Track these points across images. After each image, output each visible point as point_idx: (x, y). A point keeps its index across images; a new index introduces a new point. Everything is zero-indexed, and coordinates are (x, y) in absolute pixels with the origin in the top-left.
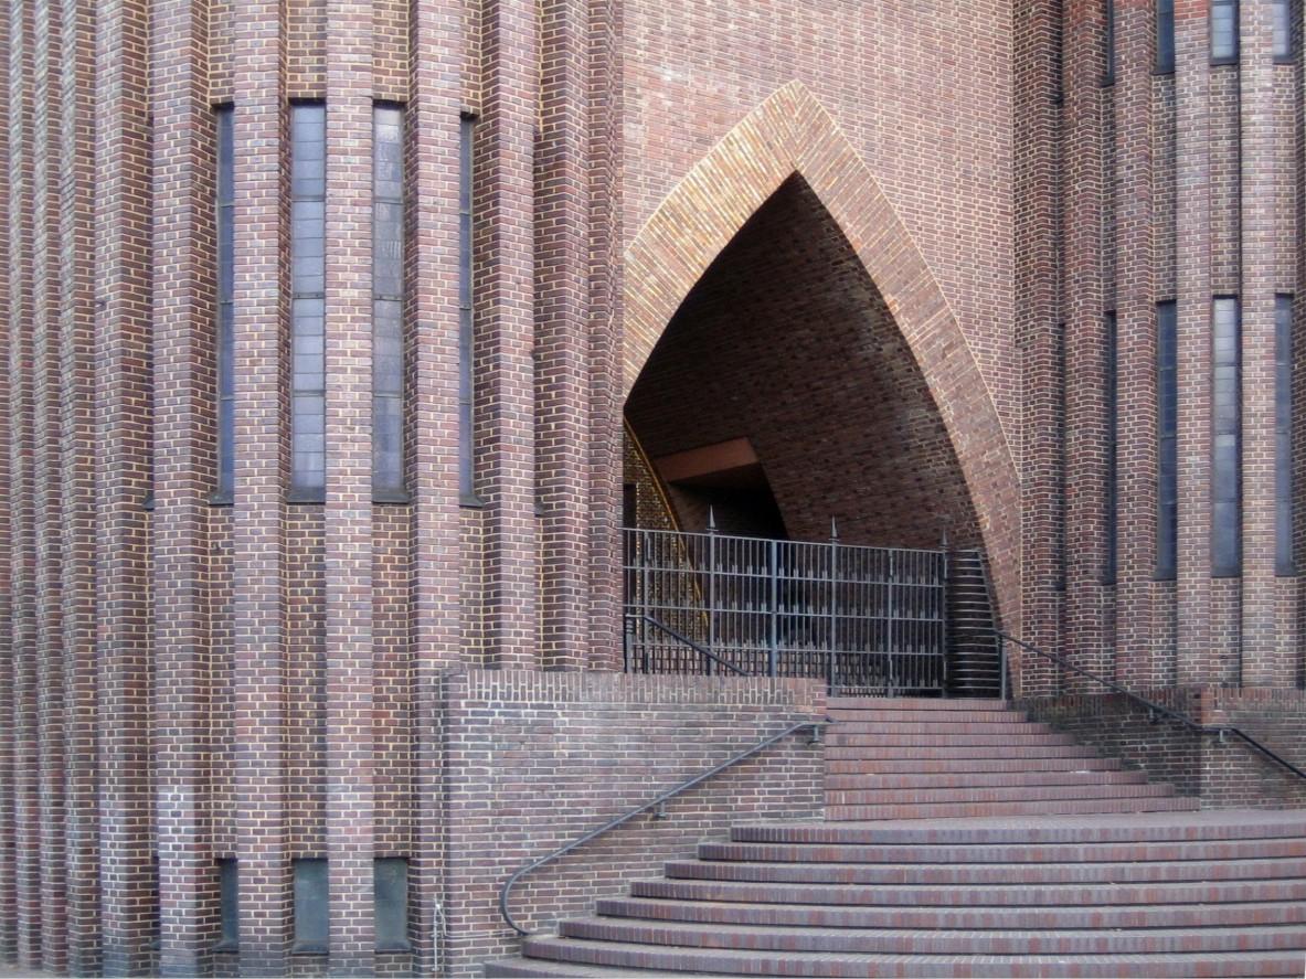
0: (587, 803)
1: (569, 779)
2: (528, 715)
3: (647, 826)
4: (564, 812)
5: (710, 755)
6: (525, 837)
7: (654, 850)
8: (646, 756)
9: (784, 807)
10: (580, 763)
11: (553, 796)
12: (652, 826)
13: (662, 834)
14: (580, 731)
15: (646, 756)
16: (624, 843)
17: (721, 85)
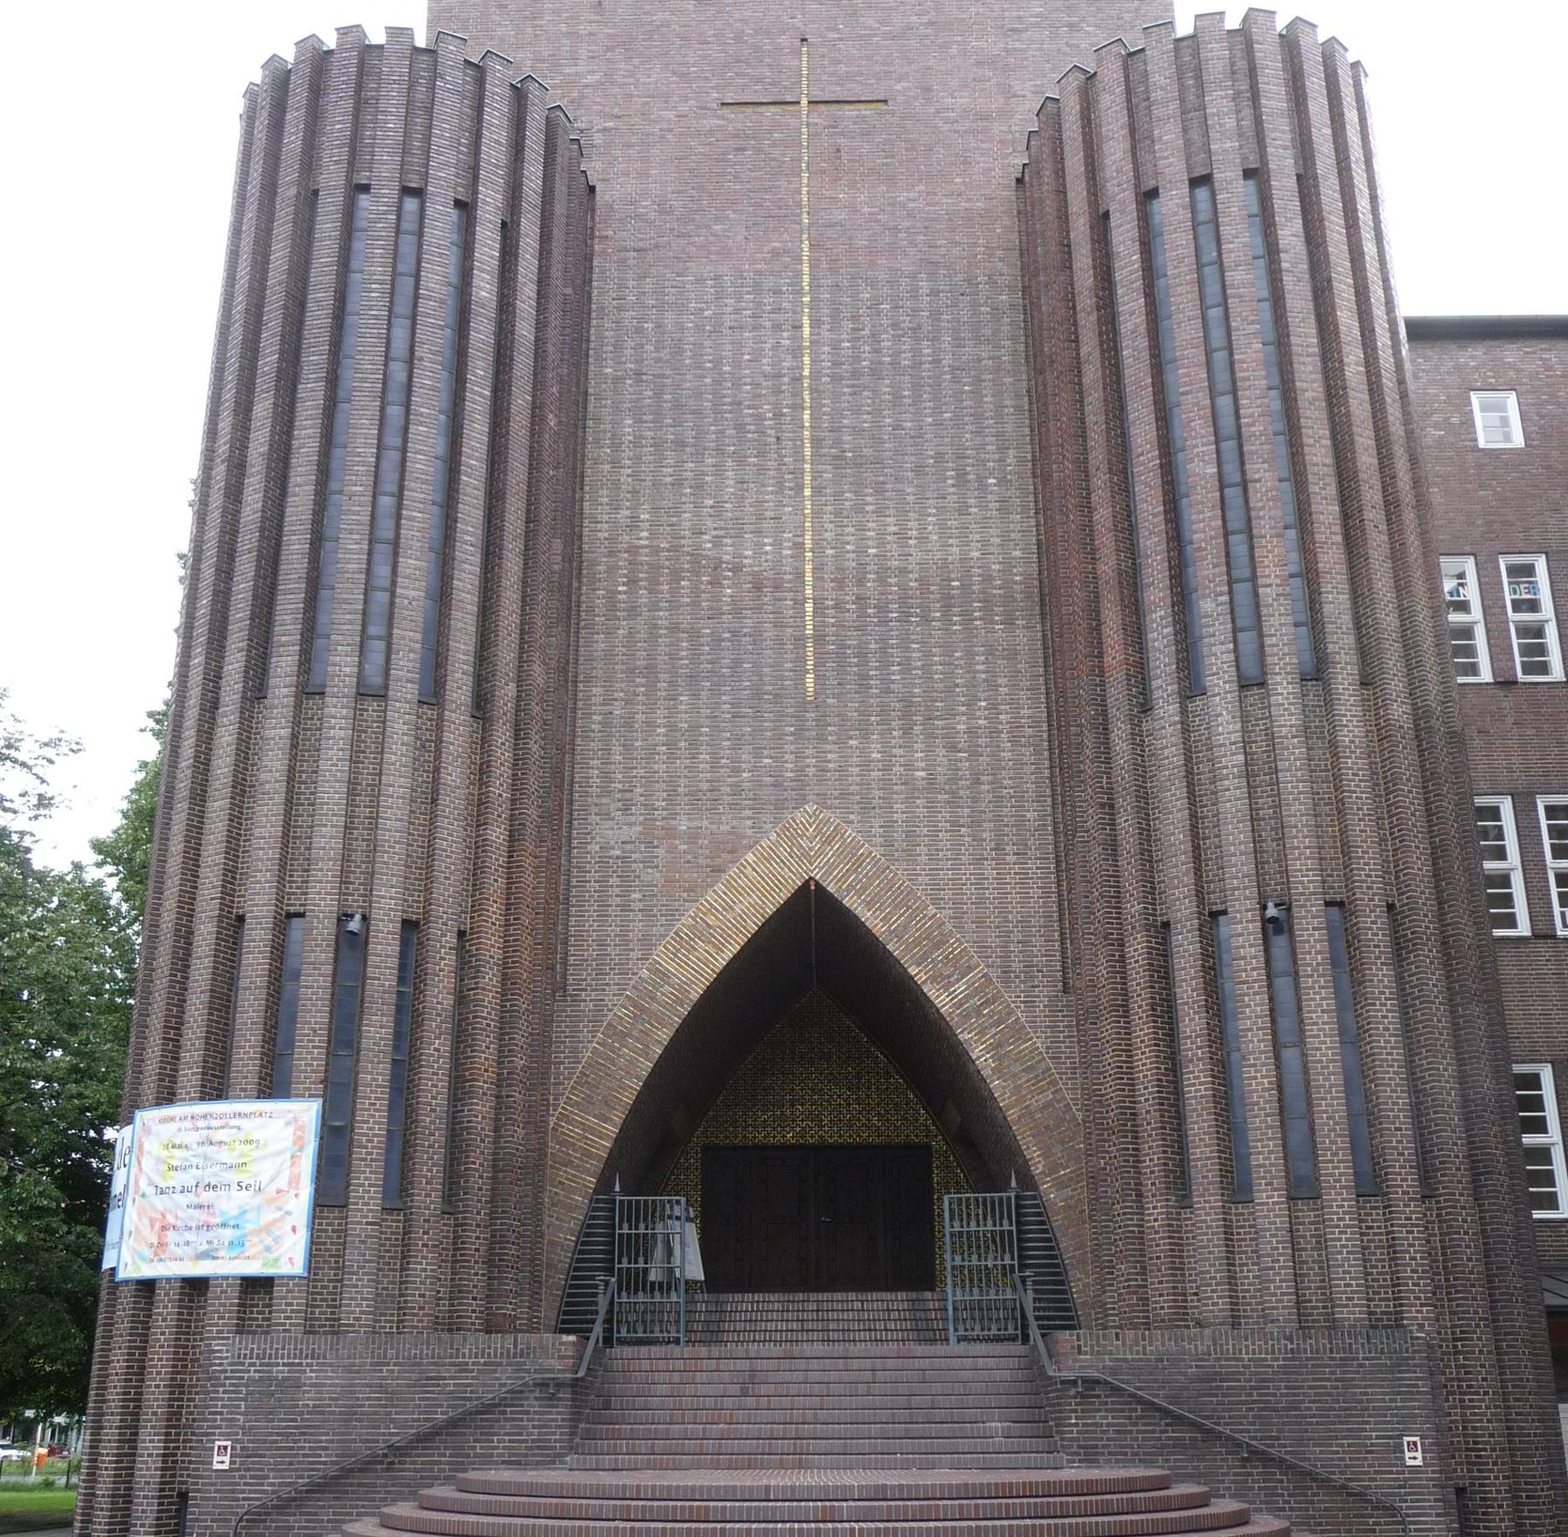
0: (326, 1448)
1: (309, 1427)
2: (280, 1371)
3: (383, 1470)
4: (305, 1456)
5: (449, 1406)
6: (267, 1477)
7: (388, 1492)
8: (385, 1406)
9: (526, 1455)
10: (322, 1413)
11: (295, 1442)
12: (388, 1470)
13: (396, 1478)
14: (324, 1385)
15: (385, 1406)
16: (359, 1485)
17: (735, 822)
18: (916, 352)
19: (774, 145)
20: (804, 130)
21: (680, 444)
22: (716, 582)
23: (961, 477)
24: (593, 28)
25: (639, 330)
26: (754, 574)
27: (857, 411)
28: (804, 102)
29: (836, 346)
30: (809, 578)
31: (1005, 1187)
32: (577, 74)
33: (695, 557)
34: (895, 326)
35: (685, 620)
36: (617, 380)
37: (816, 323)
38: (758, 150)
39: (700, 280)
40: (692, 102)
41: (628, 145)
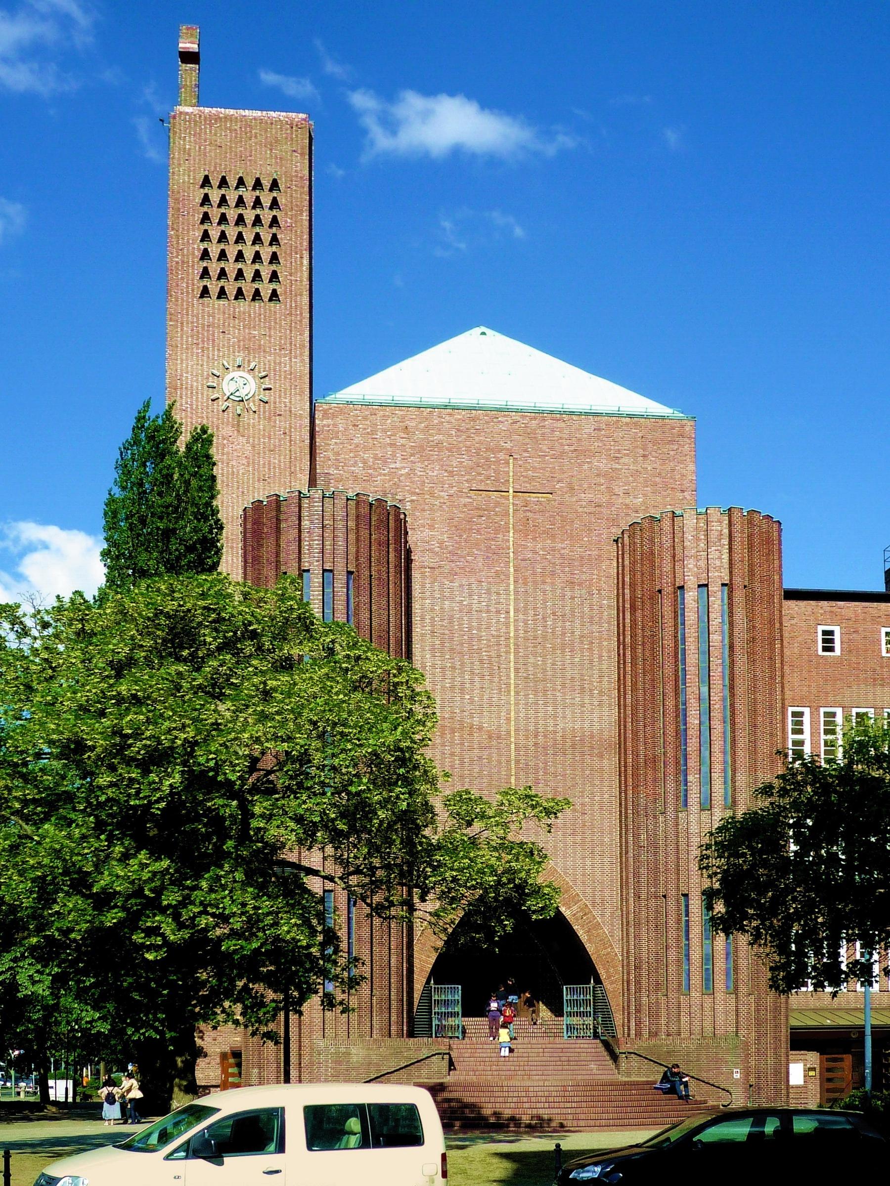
18: (564, 628)
19: (496, 515)
20: (511, 507)
21: (453, 668)
22: (471, 734)
23: (583, 689)
24: (403, 441)
25: (432, 610)
26: (488, 731)
27: (535, 655)
28: (511, 491)
29: (525, 622)
30: (513, 733)
31: (589, 983)
32: (396, 468)
33: (461, 722)
34: (554, 614)
35: (457, 750)
36: (423, 635)
37: (516, 611)
38: (489, 517)
39: (461, 586)
40: (455, 488)
41: (423, 510)
